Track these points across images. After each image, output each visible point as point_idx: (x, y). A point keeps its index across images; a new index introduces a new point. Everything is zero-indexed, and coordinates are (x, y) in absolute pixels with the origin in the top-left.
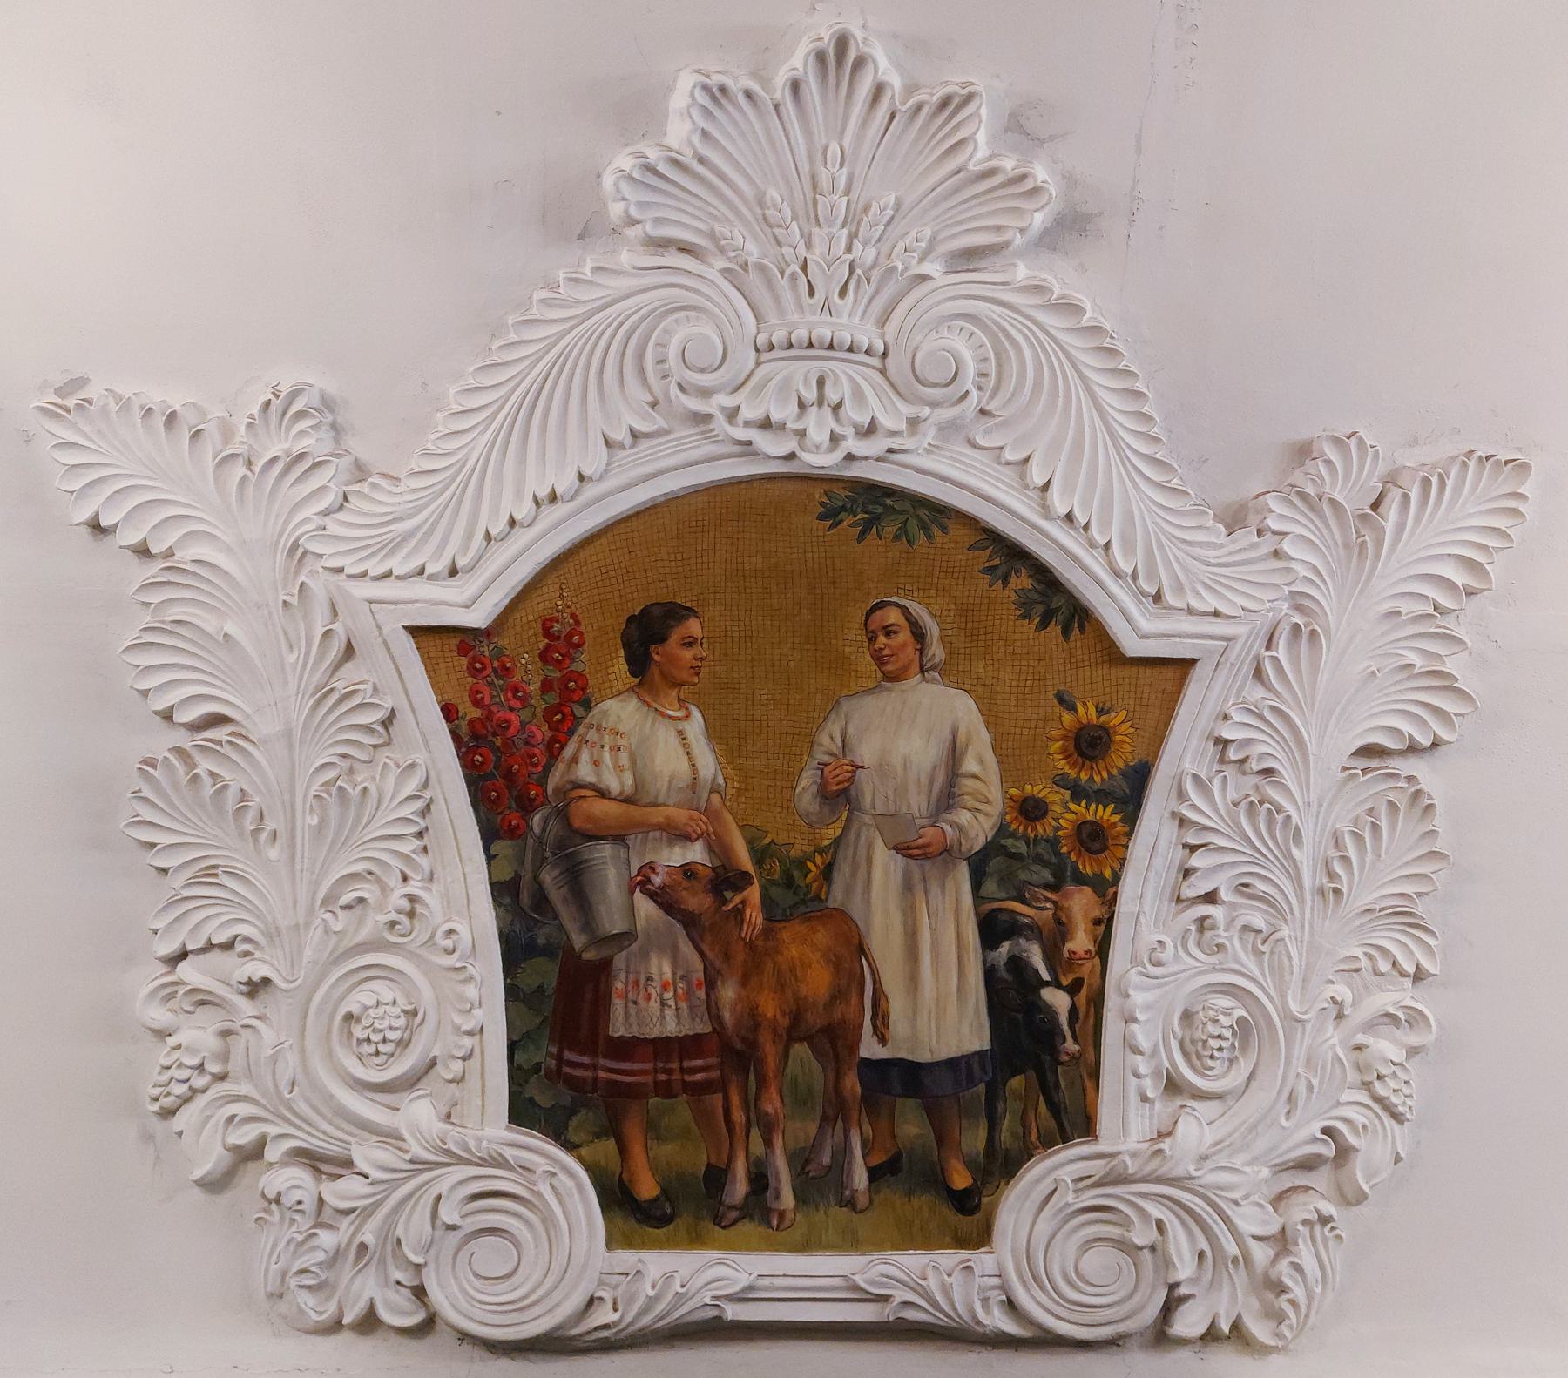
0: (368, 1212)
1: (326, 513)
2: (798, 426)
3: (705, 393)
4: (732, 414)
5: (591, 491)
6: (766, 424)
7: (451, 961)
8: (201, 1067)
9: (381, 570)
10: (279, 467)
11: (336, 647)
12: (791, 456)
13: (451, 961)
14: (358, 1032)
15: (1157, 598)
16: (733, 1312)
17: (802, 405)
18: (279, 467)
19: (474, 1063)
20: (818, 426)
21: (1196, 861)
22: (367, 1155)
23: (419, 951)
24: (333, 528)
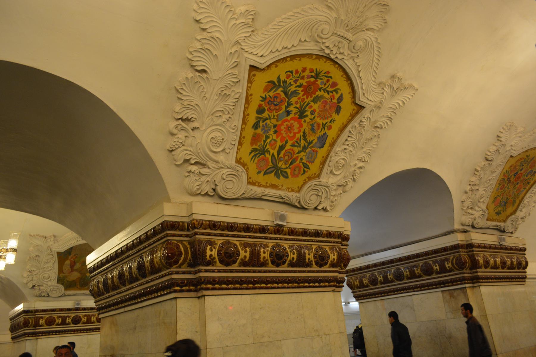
0: (210, 175)
1: (245, 37)
2: (332, 49)
3: (322, 38)
4: (323, 43)
5: (293, 49)
6: (327, 47)
7: (234, 131)
8: (181, 143)
9: (250, 52)
10: (243, 24)
11: (235, 64)
12: (328, 54)
13: (234, 131)
14: (213, 141)
15: (364, 94)
16: (264, 197)
17: (335, 45)
18: (243, 24)
19: (232, 151)
20: (335, 50)
21: (349, 139)
22: (210, 164)
23: (228, 128)
24: (246, 40)
